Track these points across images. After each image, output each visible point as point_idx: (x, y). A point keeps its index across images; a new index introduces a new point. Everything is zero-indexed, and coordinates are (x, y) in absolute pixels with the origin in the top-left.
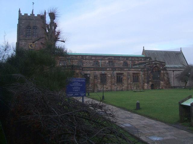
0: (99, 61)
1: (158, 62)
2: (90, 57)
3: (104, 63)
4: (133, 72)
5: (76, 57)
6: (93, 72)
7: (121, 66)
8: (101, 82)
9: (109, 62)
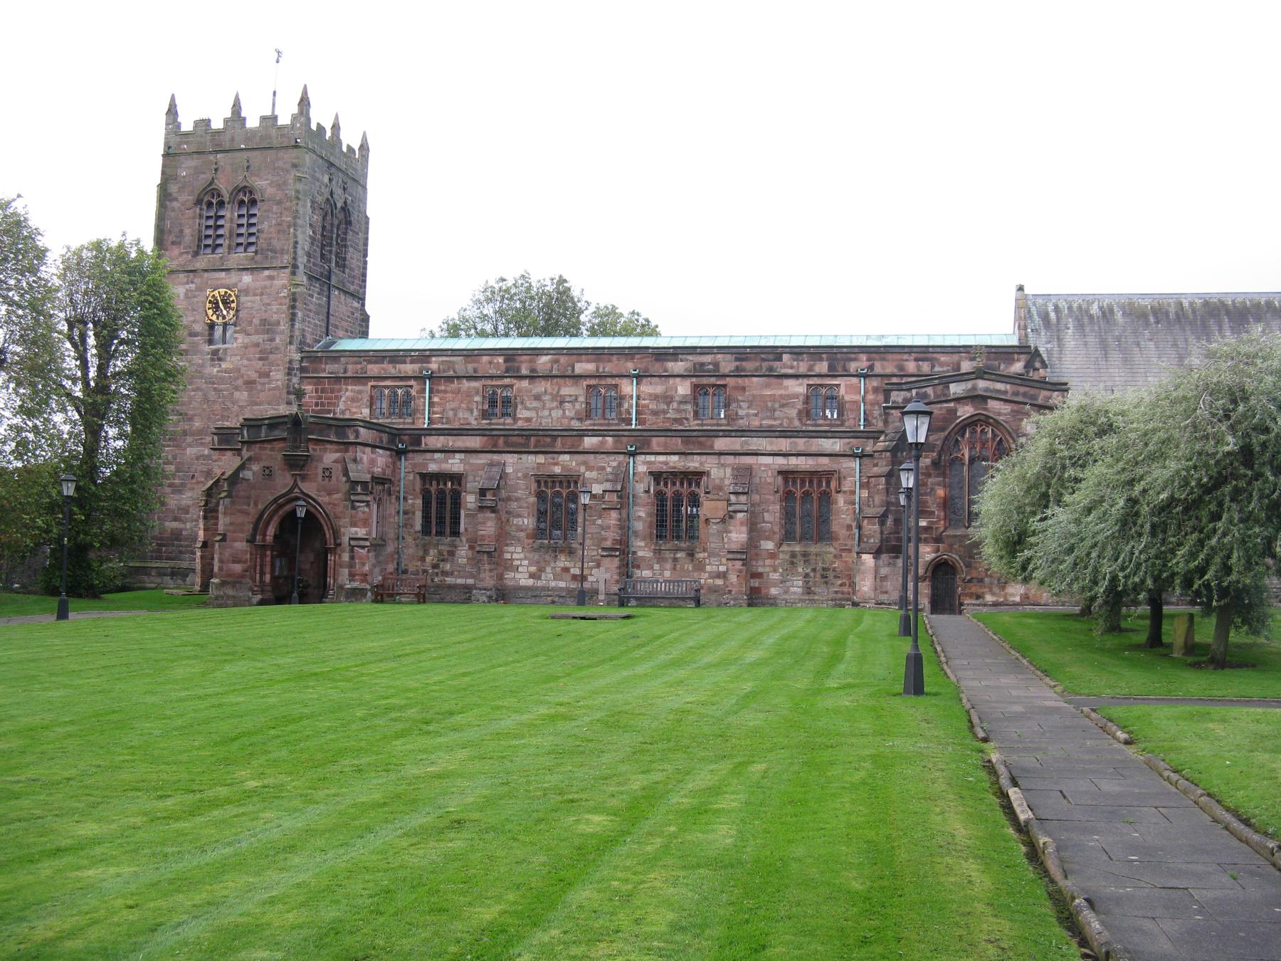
0: (629, 388)
1: (1000, 386)
2: (563, 359)
3: (655, 397)
4: (780, 461)
5: (470, 367)
6: (483, 459)
7: (790, 416)
8: (538, 533)
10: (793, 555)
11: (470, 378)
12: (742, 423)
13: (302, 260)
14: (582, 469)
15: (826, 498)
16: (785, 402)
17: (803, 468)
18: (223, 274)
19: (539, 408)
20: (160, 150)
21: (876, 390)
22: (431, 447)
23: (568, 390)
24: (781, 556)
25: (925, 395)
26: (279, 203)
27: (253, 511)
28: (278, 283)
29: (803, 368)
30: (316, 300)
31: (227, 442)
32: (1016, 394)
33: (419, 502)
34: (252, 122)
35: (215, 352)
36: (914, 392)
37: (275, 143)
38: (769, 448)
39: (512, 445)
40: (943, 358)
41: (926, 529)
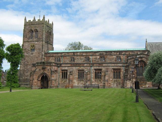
0: (90, 57)
1: (144, 56)
4: (113, 67)
7: (113, 61)
8: (79, 78)
9: (101, 57)
10: (115, 81)
11: (69, 56)
12: (107, 62)
13: (44, 40)
14: (84, 69)
15: (120, 72)
16: (113, 59)
17: (116, 68)
18: (33, 42)
19: (78, 60)
20: (24, 24)
21: (126, 57)
22: (63, 66)
23: (82, 57)
24: (113, 81)
25: (133, 57)
26: (41, 32)
27: (38, 75)
28: (41, 43)
29: (115, 54)
30: (46, 45)
31: (34, 66)
32: (147, 57)
33: (61, 74)
34: (37, 20)
35: (32, 53)
36: (132, 57)
37: (40, 23)
38: (111, 65)
39: (74, 65)
40: (135, 52)
41: (134, 77)
